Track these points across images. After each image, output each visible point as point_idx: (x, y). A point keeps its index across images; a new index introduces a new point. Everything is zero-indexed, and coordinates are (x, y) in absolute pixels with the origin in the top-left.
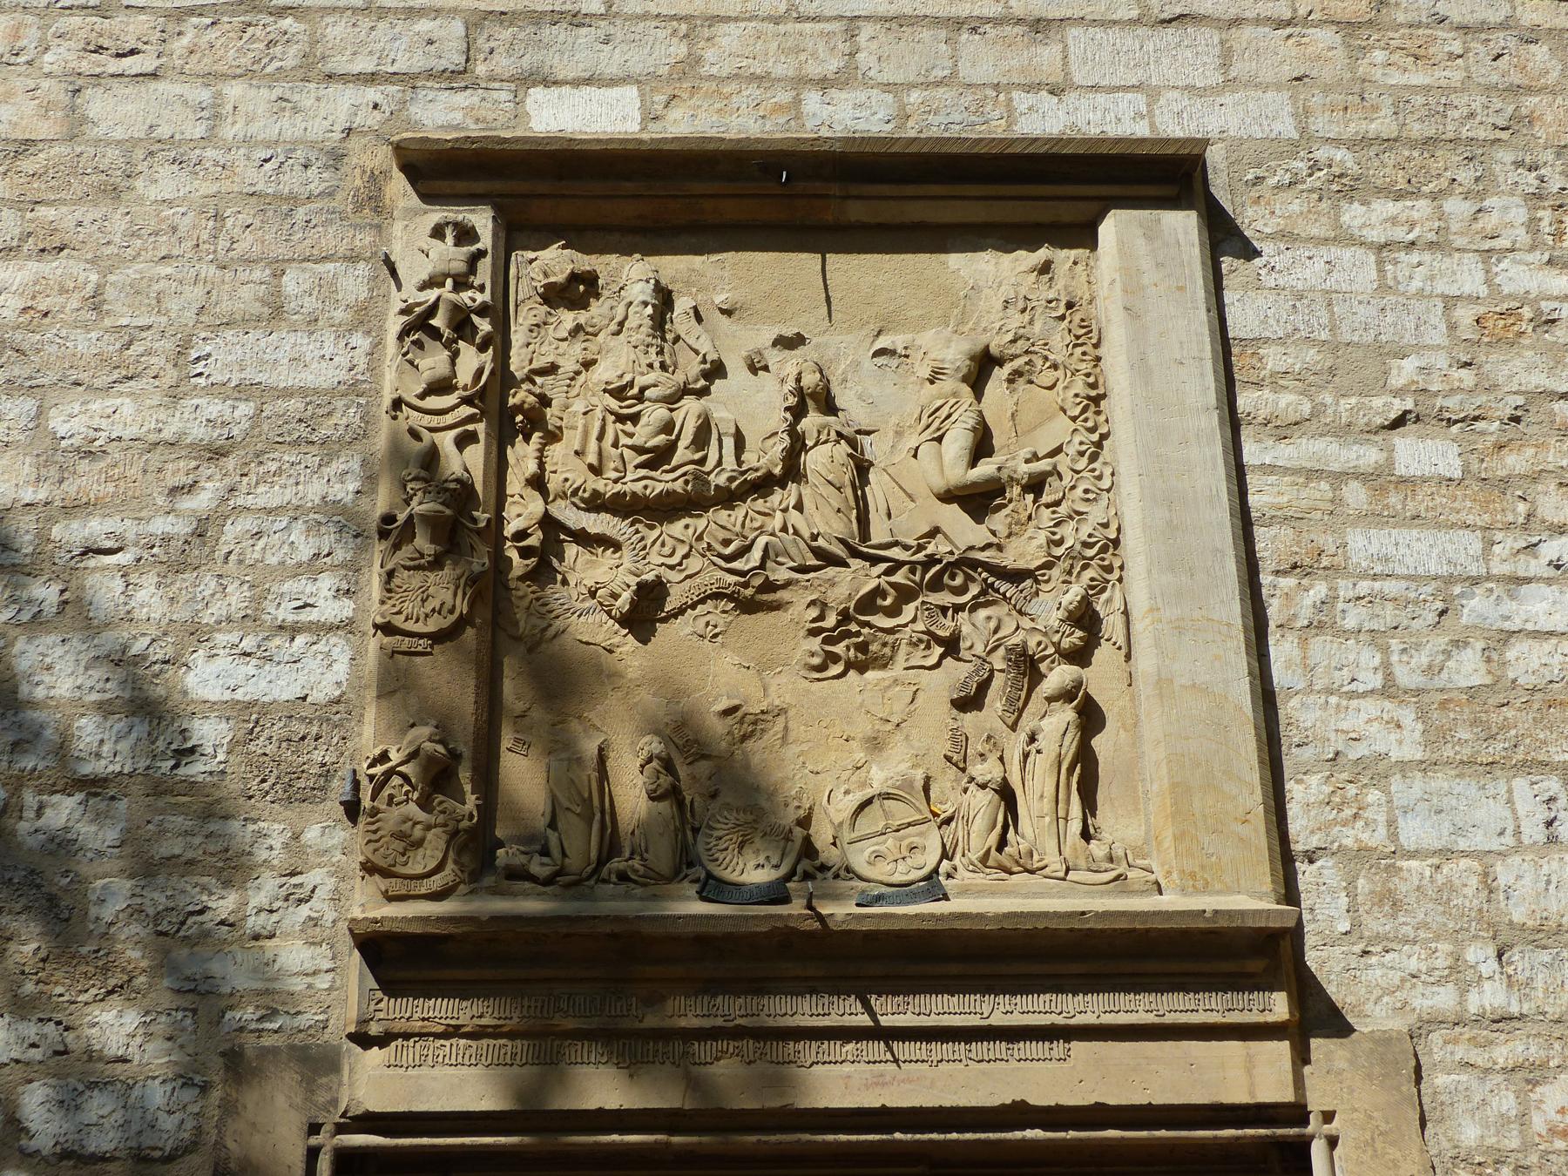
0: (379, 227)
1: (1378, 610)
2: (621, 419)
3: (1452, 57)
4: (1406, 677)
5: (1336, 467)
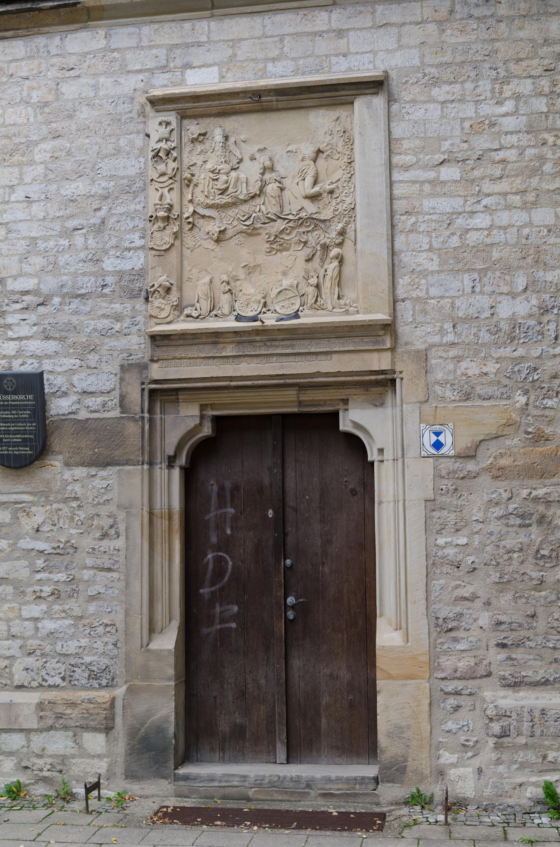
0: (145, 122)
1: (430, 225)
2: (214, 180)
3: (473, 30)
4: (436, 245)
5: (421, 179)
